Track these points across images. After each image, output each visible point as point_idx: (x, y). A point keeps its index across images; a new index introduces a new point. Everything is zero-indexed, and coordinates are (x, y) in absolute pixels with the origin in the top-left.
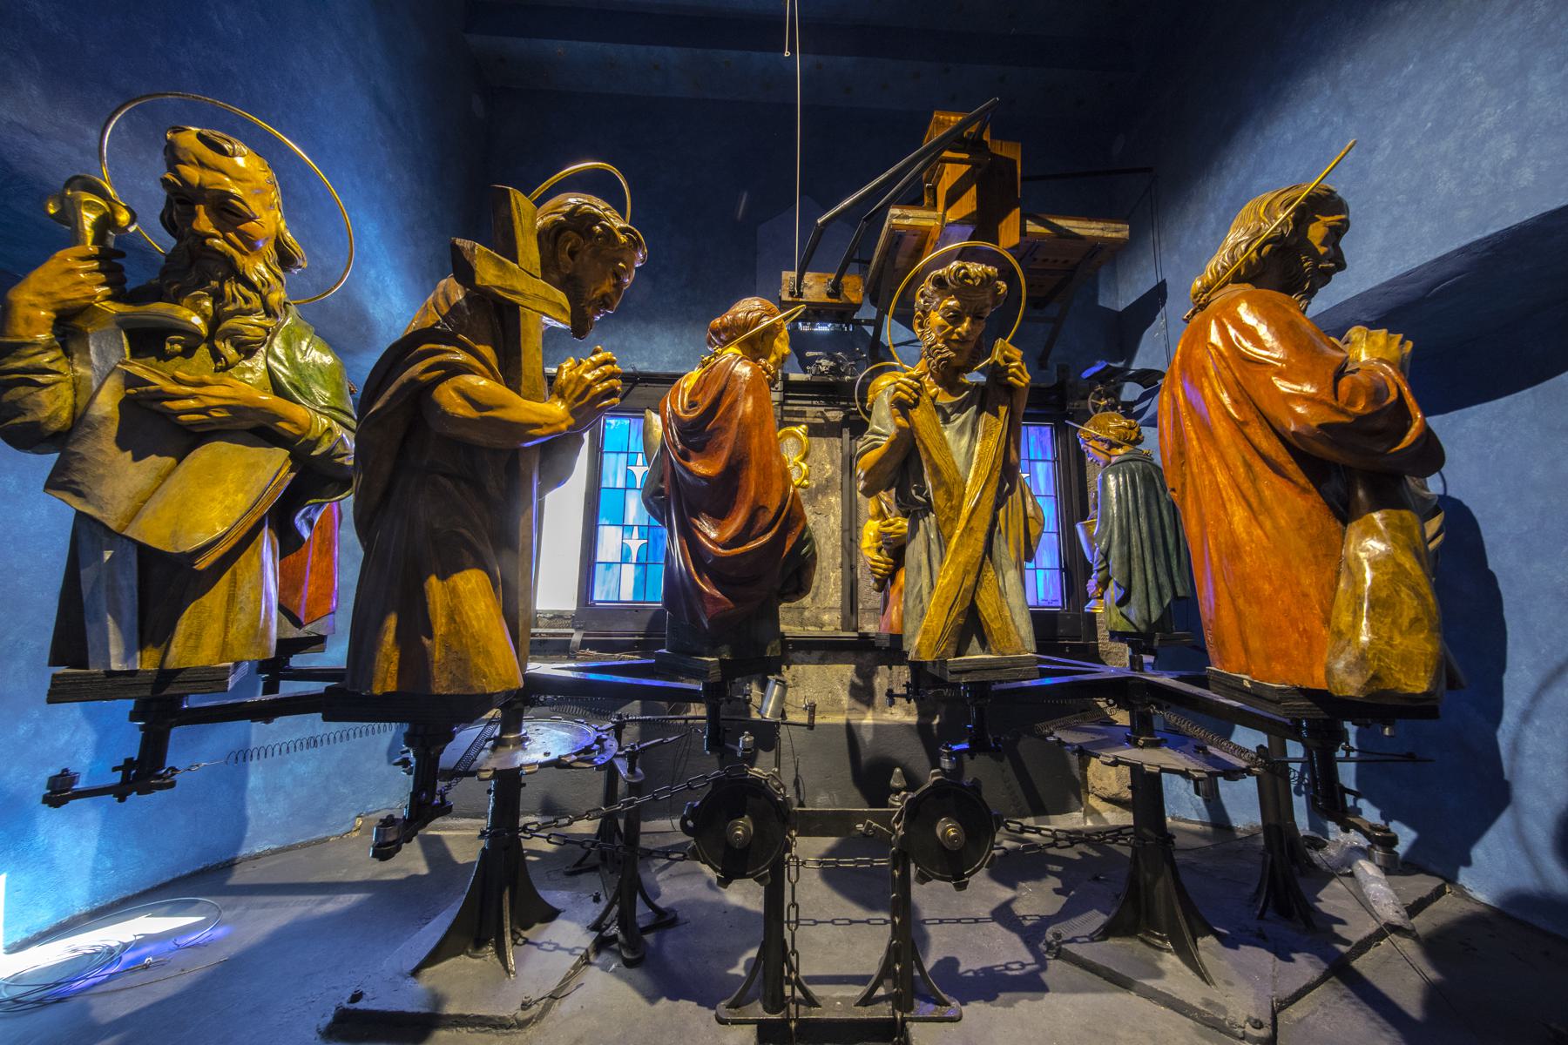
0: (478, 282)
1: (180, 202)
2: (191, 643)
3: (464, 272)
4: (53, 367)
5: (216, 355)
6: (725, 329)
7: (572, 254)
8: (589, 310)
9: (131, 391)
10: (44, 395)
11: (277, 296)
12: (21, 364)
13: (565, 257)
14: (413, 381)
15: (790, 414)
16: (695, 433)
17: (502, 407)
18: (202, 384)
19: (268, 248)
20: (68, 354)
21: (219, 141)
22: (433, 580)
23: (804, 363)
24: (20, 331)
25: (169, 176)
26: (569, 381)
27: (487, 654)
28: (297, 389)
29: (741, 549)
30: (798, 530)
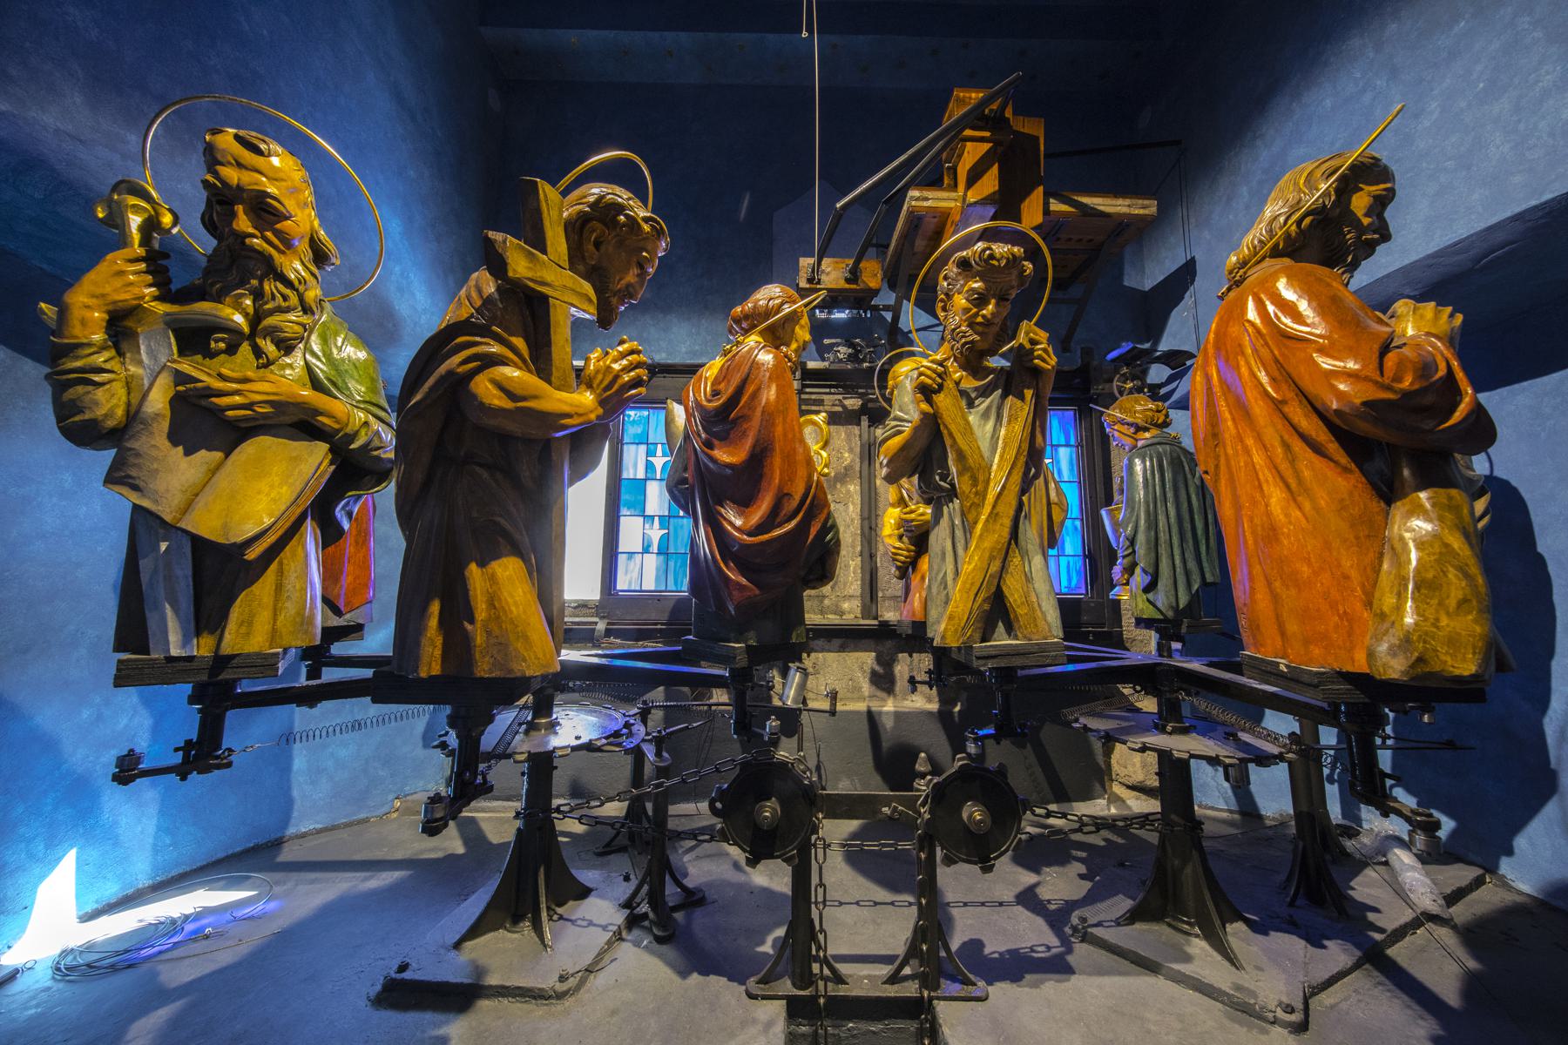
0: (510, 274)
1: (220, 203)
2: (243, 630)
3: (498, 266)
4: (108, 366)
5: (258, 352)
6: (747, 317)
7: (597, 245)
8: (614, 300)
9: (181, 388)
10: (100, 394)
11: (313, 294)
12: (78, 364)
13: (591, 247)
14: (450, 373)
15: (807, 402)
16: (722, 419)
17: (535, 397)
18: (246, 380)
19: (303, 246)
20: (120, 354)
21: (255, 142)
22: (473, 566)
23: (822, 351)
24: (77, 332)
25: (209, 177)
26: (597, 372)
27: (526, 638)
28: (334, 384)
29: (766, 537)
30: (823, 517)
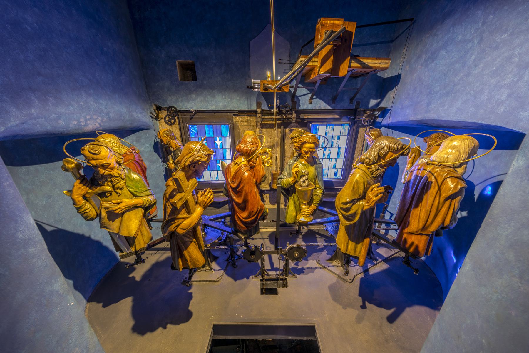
5: (117, 193)
10: (90, 213)
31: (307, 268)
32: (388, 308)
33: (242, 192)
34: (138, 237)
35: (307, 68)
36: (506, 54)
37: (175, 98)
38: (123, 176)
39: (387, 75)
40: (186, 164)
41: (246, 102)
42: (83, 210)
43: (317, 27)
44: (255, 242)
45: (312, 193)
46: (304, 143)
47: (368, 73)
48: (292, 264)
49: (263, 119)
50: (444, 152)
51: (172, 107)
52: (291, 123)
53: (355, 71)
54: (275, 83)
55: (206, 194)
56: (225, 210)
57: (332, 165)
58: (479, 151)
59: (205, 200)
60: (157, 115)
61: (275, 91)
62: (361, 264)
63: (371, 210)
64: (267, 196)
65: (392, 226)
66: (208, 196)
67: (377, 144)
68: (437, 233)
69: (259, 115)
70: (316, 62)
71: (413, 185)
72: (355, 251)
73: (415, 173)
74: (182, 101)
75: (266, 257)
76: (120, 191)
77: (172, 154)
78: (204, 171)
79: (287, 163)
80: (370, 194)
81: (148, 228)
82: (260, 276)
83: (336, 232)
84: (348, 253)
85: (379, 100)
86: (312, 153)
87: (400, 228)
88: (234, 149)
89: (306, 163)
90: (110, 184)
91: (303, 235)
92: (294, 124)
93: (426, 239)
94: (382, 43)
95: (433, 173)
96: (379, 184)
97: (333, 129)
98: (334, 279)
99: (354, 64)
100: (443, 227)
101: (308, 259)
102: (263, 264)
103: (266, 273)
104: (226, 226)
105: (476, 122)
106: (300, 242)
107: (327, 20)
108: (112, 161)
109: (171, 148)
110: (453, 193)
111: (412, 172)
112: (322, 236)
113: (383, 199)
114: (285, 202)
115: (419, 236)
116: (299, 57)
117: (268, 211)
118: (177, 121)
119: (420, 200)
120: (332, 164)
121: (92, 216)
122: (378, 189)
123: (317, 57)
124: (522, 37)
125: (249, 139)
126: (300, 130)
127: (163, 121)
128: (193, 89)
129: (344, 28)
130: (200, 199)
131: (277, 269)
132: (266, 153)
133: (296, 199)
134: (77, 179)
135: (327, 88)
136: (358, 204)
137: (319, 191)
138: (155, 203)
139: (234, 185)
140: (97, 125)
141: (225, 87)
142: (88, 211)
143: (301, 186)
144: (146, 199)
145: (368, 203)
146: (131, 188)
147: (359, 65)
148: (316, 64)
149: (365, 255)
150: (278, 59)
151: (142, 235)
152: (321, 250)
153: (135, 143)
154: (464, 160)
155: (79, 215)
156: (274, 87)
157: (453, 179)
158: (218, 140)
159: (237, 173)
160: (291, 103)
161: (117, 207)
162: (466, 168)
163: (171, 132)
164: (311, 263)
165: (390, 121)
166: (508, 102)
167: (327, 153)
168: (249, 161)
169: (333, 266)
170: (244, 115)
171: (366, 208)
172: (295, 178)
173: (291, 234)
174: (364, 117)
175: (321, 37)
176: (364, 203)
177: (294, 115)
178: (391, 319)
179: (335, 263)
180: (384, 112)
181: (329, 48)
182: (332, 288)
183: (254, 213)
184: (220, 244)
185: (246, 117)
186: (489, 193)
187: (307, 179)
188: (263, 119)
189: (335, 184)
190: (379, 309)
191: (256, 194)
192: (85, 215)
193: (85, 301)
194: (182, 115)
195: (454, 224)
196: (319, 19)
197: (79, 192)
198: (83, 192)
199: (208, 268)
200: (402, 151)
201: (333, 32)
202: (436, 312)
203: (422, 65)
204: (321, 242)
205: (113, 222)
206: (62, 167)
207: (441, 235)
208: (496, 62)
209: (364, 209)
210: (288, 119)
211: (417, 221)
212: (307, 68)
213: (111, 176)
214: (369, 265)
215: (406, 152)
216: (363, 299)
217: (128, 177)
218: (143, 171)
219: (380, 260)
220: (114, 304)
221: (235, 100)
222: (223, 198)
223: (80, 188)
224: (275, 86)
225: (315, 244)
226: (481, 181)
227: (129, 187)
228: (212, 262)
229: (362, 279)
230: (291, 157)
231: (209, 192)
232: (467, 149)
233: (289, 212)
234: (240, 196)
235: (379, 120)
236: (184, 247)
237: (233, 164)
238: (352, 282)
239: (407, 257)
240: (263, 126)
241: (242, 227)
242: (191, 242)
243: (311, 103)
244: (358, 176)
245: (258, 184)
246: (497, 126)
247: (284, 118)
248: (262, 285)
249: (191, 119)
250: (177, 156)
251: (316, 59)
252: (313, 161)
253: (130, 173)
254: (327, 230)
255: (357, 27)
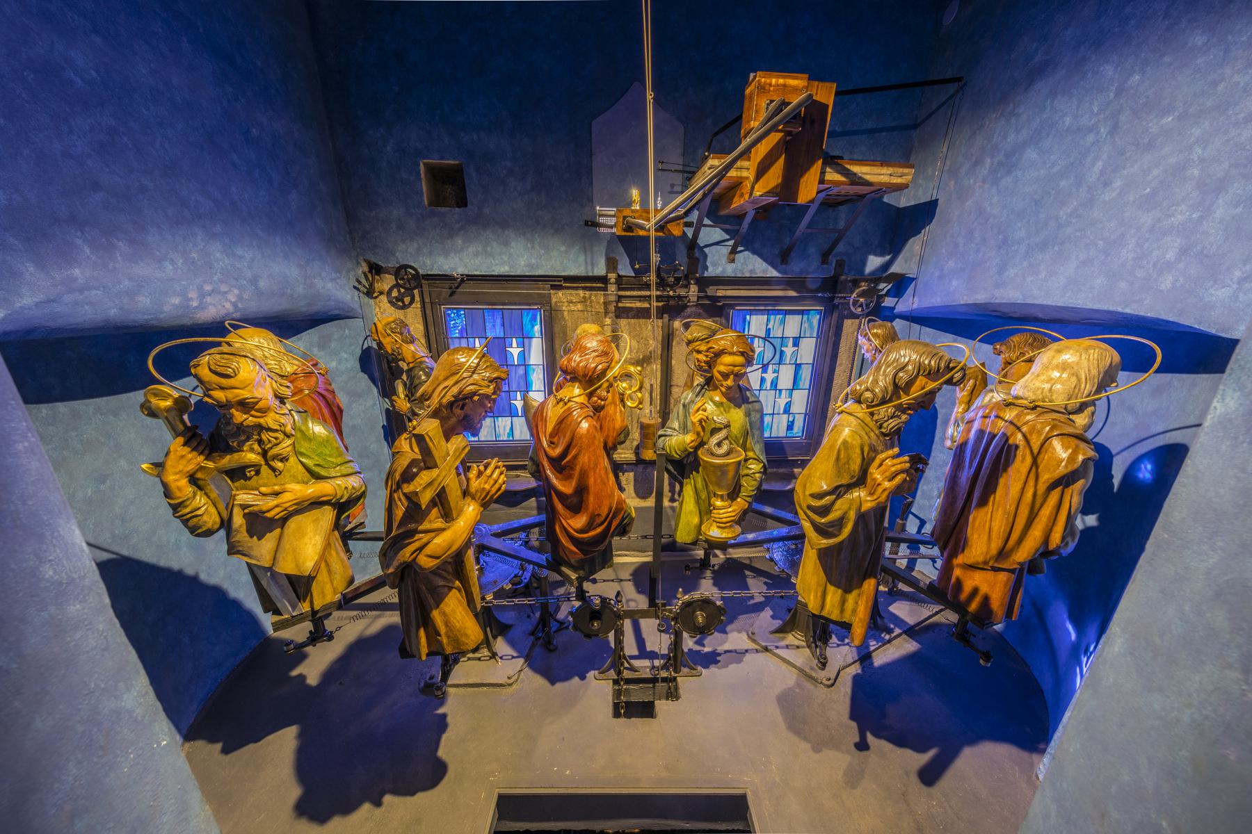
5: (273, 469)
10: (205, 518)
31: (726, 652)
32: (921, 749)
33: (572, 469)
34: (319, 577)
35: (724, 183)
36: (1172, 160)
37: (415, 245)
38: (289, 429)
39: (904, 201)
40: (444, 401)
41: (582, 258)
42: (188, 510)
43: (748, 91)
44: (602, 587)
45: (737, 471)
46: (722, 352)
47: (862, 196)
48: (689, 643)
49: (620, 298)
50: (1043, 378)
51: (406, 267)
52: (686, 306)
53: (835, 191)
54: (652, 215)
55: (488, 472)
56: (529, 512)
57: (783, 403)
58: (1122, 375)
59: (487, 487)
60: (371, 285)
61: (653, 234)
62: (857, 642)
63: (879, 511)
64: (628, 478)
65: (923, 549)
66: (494, 477)
67: (889, 358)
68: (1032, 567)
69: (612, 288)
70: (745, 170)
71: (974, 451)
72: (842, 611)
73: (976, 426)
74: (430, 253)
75: (627, 624)
76: (279, 465)
77: (404, 377)
78: (484, 418)
79: (677, 401)
80: (876, 474)
81: (343, 555)
82: (612, 671)
83: (794, 565)
84: (824, 614)
85: (888, 257)
86: (738, 376)
87: (945, 554)
88: (551, 366)
89: (725, 400)
90: (256, 446)
91: (714, 572)
92: (693, 309)
93: (1008, 580)
94: (891, 129)
95: (1019, 424)
96: (896, 450)
97: (783, 322)
98: (790, 678)
99: (832, 176)
100: (1046, 551)
101: (729, 628)
102: (619, 642)
103: (626, 665)
104: (531, 548)
105: (1111, 308)
106: (707, 589)
107: (771, 77)
108: (264, 392)
109: (401, 363)
110: (1066, 471)
111: (971, 422)
112: (759, 573)
113: (906, 485)
114: (672, 490)
115: (990, 575)
116: (706, 158)
117: (634, 515)
118: (417, 298)
119: (990, 488)
120: (782, 402)
121: (209, 525)
122: (895, 461)
123: (749, 159)
124: (1207, 123)
125: (592, 344)
126: (708, 322)
127: (384, 298)
128: (457, 226)
129: (810, 96)
130: (475, 485)
131: (652, 655)
132: (628, 376)
133: (700, 484)
134: (177, 434)
135: (769, 227)
136: (848, 496)
137: (755, 467)
138: (363, 495)
139: (556, 452)
140: (228, 306)
141: (535, 222)
142: (199, 512)
143: (713, 454)
144: (340, 485)
145: (871, 494)
146: (308, 457)
147: (843, 179)
148: (745, 174)
149: (867, 618)
150: (659, 161)
151: (329, 571)
152: (758, 608)
153: (315, 351)
154: (1089, 395)
155: (177, 523)
156: (651, 224)
157: (1066, 439)
158: (514, 344)
159: (561, 422)
160: (686, 260)
161: (272, 502)
162: (1093, 414)
163: (403, 325)
164: (735, 639)
165: (915, 306)
166: (1181, 266)
167: (769, 376)
168: (590, 395)
169: (787, 647)
170: (577, 288)
171: (866, 506)
172: (698, 434)
173: (687, 568)
174: (854, 295)
175: (756, 116)
176: (862, 494)
177: (694, 289)
178: (929, 775)
179: (791, 639)
180: (901, 284)
181: (775, 137)
182: (786, 701)
183: (602, 519)
184: (514, 594)
185: (581, 292)
186: (1148, 476)
187: (726, 438)
188: (620, 298)
189: (789, 451)
190: (899, 751)
191: (607, 473)
192: (191, 523)
193: (178, 738)
194: (429, 286)
195: (1072, 545)
196: (752, 75)
197: (181, 467)
198: (191, 467)
199: (485, 652)
200: (947, 374)
201: (784, 104)
202: (1035, 757)
203: (984, 181)
204: (757, 589)
205: (259, 539)
206: (142, 406)
207: (1041, 572)
208: (1149, 178)
209: (863, 509)
210: (680, 297)
211: (986, 537)
212: (724, 183)
213: (261, 428)
214: (873, 644)
215: (958, 376)
216: (859, 727)
217: (301, 431)
218: (335, 416)
219: (897, 631)
220: (251, 746)
221: (555, 253)
222: (526, 481)
223: (182, 457)
224: (653, 221)
225: (743, 594)
226: (1127, 445)
227: (302, 454)
228: (495, 637)
229: (856, 679)
230: (686, 384)
231: (496, 467)
232: (1094, 372)
233: (683, 515)
234: (569, 477)
235: (888, 302)
236: (432, 601)
237: (552, 400)
238: (833, 685)
239: (963, 622)
240: (621, 313)
241: (571, 551)
242: (451, 588)
243: (733, 261)
244: (847, 431)
245: (609, 449)
246: (1158, 319)
247: (669, 297)
248: (618, 693)
249: (451, 295)
250: (417, 382)
251: (746, 164)
252: (739, 396)
253: (305, 421)
254: (772, 560)
255: (837, 94)
